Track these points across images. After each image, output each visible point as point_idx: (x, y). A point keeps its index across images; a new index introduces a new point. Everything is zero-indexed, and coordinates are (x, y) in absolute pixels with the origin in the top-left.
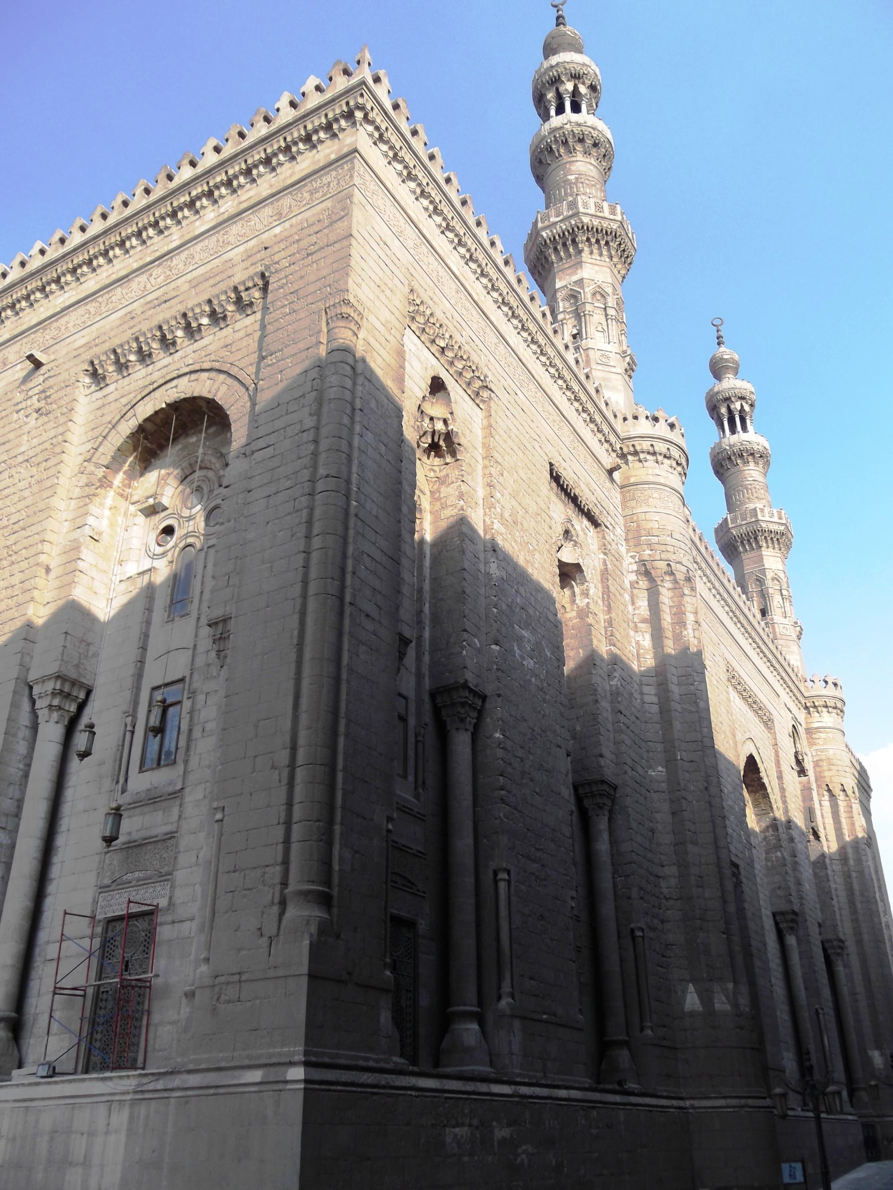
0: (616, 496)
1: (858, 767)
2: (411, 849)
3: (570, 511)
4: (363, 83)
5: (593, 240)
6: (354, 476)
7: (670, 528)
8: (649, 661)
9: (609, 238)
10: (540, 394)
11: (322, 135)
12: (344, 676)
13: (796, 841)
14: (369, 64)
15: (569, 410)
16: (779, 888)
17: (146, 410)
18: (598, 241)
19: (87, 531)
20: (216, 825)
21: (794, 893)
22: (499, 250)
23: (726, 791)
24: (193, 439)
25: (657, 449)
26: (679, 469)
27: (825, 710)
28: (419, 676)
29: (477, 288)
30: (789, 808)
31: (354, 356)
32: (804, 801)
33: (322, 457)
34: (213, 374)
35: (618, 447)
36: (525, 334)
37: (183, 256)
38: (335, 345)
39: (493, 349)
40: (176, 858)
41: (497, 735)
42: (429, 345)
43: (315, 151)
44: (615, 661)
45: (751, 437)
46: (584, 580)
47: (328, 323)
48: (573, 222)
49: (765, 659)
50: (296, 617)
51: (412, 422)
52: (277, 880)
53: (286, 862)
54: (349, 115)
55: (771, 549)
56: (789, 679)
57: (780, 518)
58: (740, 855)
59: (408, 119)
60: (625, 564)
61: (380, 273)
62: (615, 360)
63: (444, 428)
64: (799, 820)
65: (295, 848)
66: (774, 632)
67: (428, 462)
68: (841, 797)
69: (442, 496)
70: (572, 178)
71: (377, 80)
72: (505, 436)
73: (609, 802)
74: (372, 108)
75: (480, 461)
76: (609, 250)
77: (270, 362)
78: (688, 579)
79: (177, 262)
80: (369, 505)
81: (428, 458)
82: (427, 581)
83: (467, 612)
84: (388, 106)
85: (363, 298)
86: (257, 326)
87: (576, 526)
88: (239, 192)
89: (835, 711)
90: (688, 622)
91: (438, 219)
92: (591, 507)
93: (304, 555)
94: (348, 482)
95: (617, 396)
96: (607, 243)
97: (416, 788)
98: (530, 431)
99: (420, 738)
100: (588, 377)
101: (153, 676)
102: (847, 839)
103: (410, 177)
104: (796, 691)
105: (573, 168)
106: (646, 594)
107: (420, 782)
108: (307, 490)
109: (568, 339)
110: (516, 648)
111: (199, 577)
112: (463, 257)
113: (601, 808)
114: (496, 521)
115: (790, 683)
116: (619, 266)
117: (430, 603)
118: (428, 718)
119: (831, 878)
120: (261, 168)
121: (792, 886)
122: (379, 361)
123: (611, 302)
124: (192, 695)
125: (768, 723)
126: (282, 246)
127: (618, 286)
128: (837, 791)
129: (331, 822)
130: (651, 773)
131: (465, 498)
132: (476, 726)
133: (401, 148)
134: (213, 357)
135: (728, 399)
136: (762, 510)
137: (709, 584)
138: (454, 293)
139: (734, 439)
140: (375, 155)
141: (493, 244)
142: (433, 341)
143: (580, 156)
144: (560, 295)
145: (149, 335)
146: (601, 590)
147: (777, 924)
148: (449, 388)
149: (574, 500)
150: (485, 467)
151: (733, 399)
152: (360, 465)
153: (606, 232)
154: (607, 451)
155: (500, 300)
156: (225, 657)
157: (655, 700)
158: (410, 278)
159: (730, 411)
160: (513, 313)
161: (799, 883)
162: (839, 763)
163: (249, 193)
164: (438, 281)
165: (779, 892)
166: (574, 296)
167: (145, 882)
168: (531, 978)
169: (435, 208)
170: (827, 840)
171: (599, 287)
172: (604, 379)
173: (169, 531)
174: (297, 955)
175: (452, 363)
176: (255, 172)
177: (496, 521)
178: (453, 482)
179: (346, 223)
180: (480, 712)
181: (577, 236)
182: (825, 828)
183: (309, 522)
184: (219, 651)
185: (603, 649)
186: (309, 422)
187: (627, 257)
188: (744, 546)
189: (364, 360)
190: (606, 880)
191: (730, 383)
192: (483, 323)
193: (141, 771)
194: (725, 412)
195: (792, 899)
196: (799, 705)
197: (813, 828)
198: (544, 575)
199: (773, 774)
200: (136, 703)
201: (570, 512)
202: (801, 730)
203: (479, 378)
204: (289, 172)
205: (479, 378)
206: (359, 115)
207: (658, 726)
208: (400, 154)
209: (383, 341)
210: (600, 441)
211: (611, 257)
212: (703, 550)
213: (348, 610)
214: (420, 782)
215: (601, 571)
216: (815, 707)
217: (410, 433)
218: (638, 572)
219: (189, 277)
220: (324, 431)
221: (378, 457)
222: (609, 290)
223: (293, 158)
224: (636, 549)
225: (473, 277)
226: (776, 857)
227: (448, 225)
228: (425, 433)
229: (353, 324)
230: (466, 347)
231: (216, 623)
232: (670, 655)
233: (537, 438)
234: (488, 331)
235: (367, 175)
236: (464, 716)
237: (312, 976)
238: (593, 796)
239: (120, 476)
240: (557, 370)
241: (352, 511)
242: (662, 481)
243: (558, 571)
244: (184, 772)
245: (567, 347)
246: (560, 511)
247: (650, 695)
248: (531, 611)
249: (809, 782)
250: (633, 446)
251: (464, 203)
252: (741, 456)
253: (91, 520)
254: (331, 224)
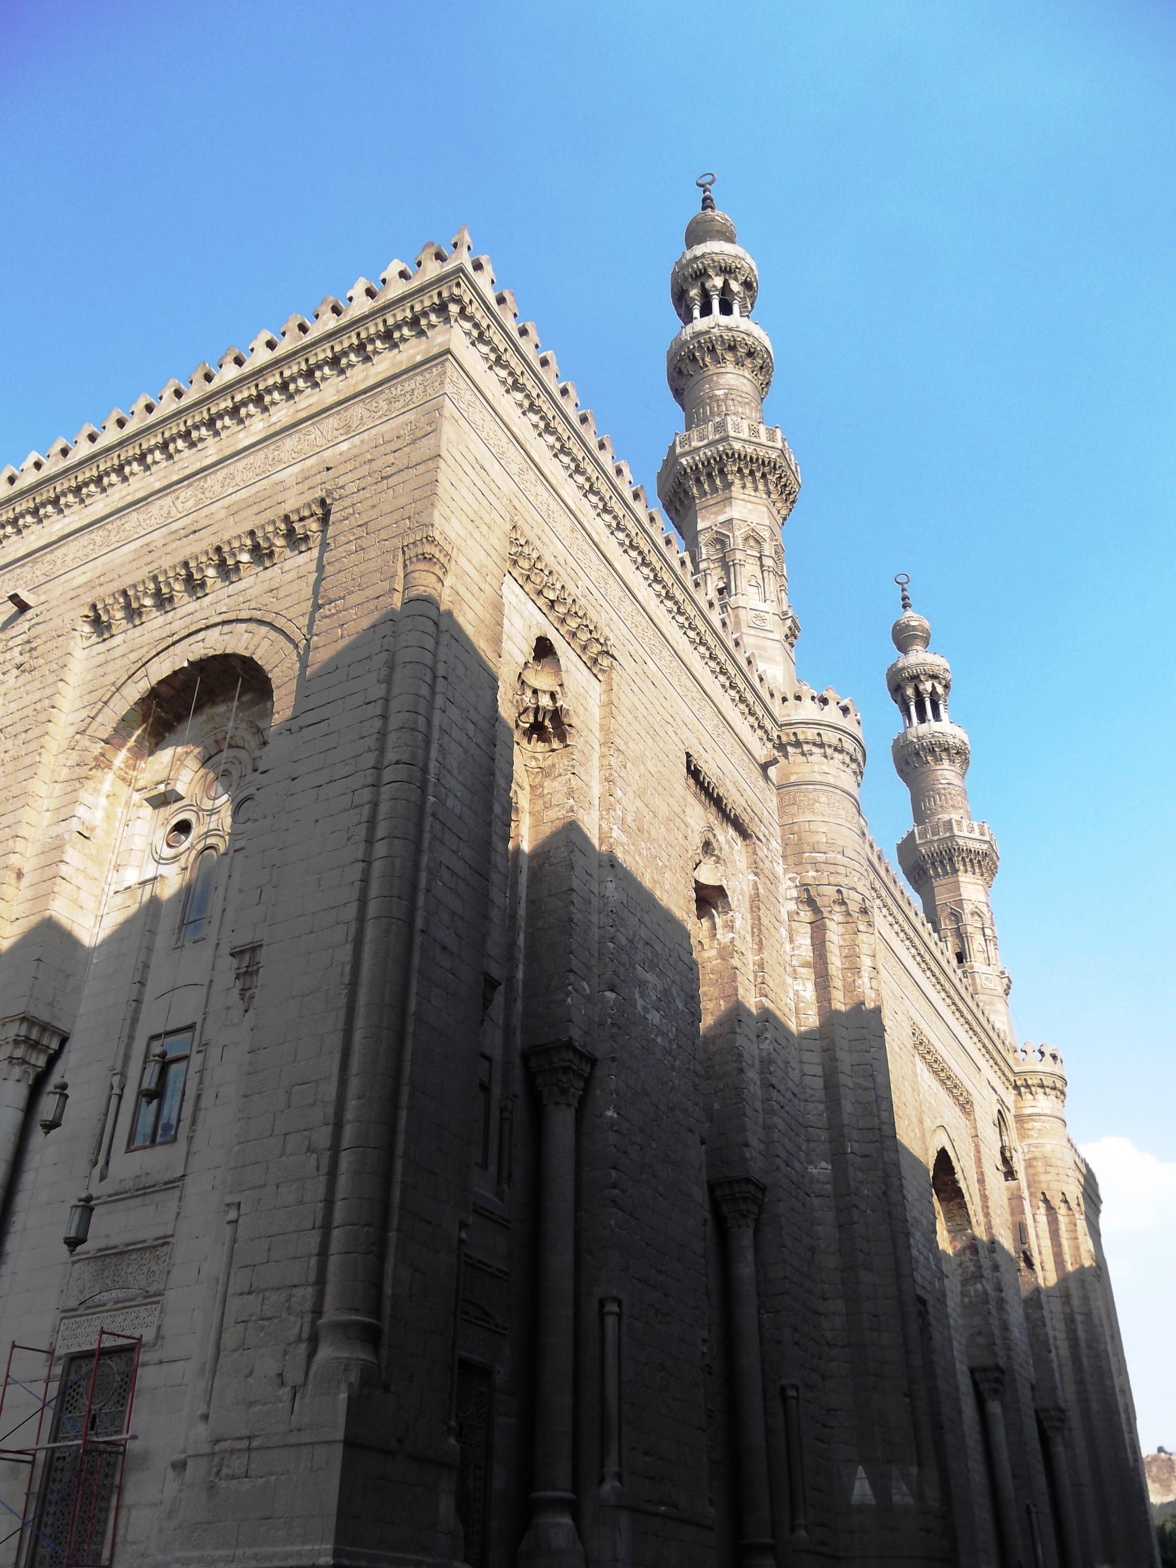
0: (772, 800)
1: (1084, 1171)
2: (490, 1267)
3: (712, 817)
4: (460, 270)
5: (746, 471)
6: (433, 766)
7: (841, 843)
8: (812, 1020)
9: (767, 469)
10: (676, 663)
11: (406, 331)
12: (410, 1028)
13: (1001, 1269)
14: (469, 248)
15: (713, 685)
16: (979, 1334)
17: (162, 669)
18: (752, 473)
19: (75, 824)
20: (229, 1228)
21: (998, 1342)
22: (627, 480)
23: (909, 1197)
24: (221, 709)
25: (825, 739)
26: (854, 766)
27: (1040, 1090)
28: (508, 1030)
29: (598, 527)
30: (993, 1222)
31: (438, 609)
32: (1012, 1214)
33: (392, 738)
34: (252, 626)
35: (775, 734)
36: (658, 587)
37: (221, 475)
38: (414, 593)
39: (616, 604)
40: (169, 1272)
41: (610, 1113)
42: (534, 597)
43: (396, 351)
44: (767, 1017)
45: (945, 727)
46: (728, 908)
47: (405, 566)
48: (721, 449)
49: (962, 1020)
50: (349, 947)
51: (510, 696)
52: (308, 1306)
53: (320, 1282)
54: (441, 309)
55: (970, 874)
56: (994, 1048)
57: (982, 834)
58: (929, 1288)
59: (515, 315)
60: (782, 888)
61: (476, 506)
62: (772, 622)
63: (551, 703)
64: (1006, 1241)
65: (334, 1262)
66: (974, 984)
67: (529, 747)
68: (1062, 1210)
69: (546, 792)
70: (719, 393)
71: (478, 266)
72: (630, 717)
73: (755, 1210)
74: (471, 301)
75: (597, 747)
76: (766, 485)
77: (328, 613)
78: (864, 911)
79: (214, 482)
80: (450, 802)
81: (529, 742)
82: (523, 905)
83: (574, 947)
84: (492, 300)
85: (452, 535)
86: (313, 566)
87: (718, 837)
88: (297, 398)
89: (1053, 1092)
90: (863, 968)
91: (551, 439)
92: (738, 811)
93: (361, 865)
94: (425, 770)
95: (775, 668)
96: (764, 476)
97: (499, 1182)
98: (662, 711)
99: (507, 1115)
100: (737, 644)
101: (152, 1021)
103: (517, 386)
104: (1002, 1064)
105: (722, 381)
106: (808, 928)
107: (505, 1174)
108: (369, 781)
109: (713, 594)
110: (637, 996)
111: (221, 890)
112: (581, 488)
113: (744, 1216)
114: (615, 827)
115: (995, 1054)
116: (779, 505)
117: (526, 932)
118: (518, 1087)
119: (1048, 1322)
120: (326, 370)
121: (996, 1331)
122: (470, 615)
123: (768, 549)
124: (204, 1048)
125: (966, 1106)
126: (350, 466)
127: (777, 530)
128: (1056, 1202)
129: (384, 1227)
130: (811, 1169)
131: (576, 796)
132: (582, 1101)
133: (506, 350)
134: (253, 605)
135: (915, 678)
136: (959, 823)
137: (890, 918)
138: (568, 532)
139: (923, 729)
140: (473, 358)
141: (619, 472)
142: (540, 593)
143: (730, 367)
144: (702, 539)
145: (171, 574)
146: (750, 922)
147: (975, 1384)
148: (559, 652)
149: (716, 802)
150: (603, 756)
151: (922, 678)
152: (442, 749)
153: (763, 461)
154: (761, 739)
155: (627, 543)
156: (252, 997)
157: (819, 1070)
158: (514, 512)
159: (918, 693)
160: (644, 559)
161: (1005, 1327)
162: (1059, 1163)
163: (310, 400)
164: (549, 516)
166: (720, 541)
167: (123, 1305)
168: (646, 1453)
169: (547, 425)
170: (1043, 1268)
171: (753, 530)
172: (758, 647)
173: (183, 827)
174: (330, 1413)
175: (563, 621)
176: (318, 374)
177: (615, 827)
178: (560, 775)
179: (432, 441)
180: (588, 1081)
181: (726, 465)
182: (1040, 1253)
183: (372, 822)
184: (242, 990)
185: (752, 1001)
186: (378, 691)
187: (790, 494)
188: (935, 869)
189: (449, 614)
190: (748, 1315)
191: (918, 657)
192: (604, 570)
193: (128, 1150)
194: (912, 694)
195: (997, 1349)
196: (1007, 1084)
197: (1024, 1253)
198: (678, 901)
199: (973, 1175)
200: (127, 1058)
201: (712, 819)
202: (1009, 1117)
203: (597, 640)
204: (361, 375)
205: (597, 640)
206: (454, 309)
207: (821, 1107)
208: (504, 358)
209: (476, 590)
210: (752, 727)
211: (769, 493)
212: (883, 873)
213: (418, 940)
214: (505, 1174)
215: (751, 896)
216: (1028, 1086)
217: (507, 711)
218: (798, 900)
219: (227, 501)
220: (395, 705)
221: (464, 739)
222: (766, 534)
223: (367, 359)
224: (798, 869)
225: (593, 513)
226: (976, 1290)
227: (563, 446)
228: (526, 710)
229: (437, 567)
230: (582, 601)
231: (242, 952)
232: (838, 1012)
233: (671, 720)
234: (611, 580)
235: (461, 381)
236: (566, 1086)
237: (350, 1444)
238: (736, 1199)
239: (123, 754)
240: (698, 634)
241: (429, 809)
242: (832, 780)
243: (694, 895)
244: (188, 1153)
245: (711, 605)
246: (698, 816)
247: (813, 1065)
248: (658, 947)
249: (1019, 1189)
250: (795, 734)
251: (584, 419)
252: (932, 752)
253: (80, 811)
254: (414, 442)
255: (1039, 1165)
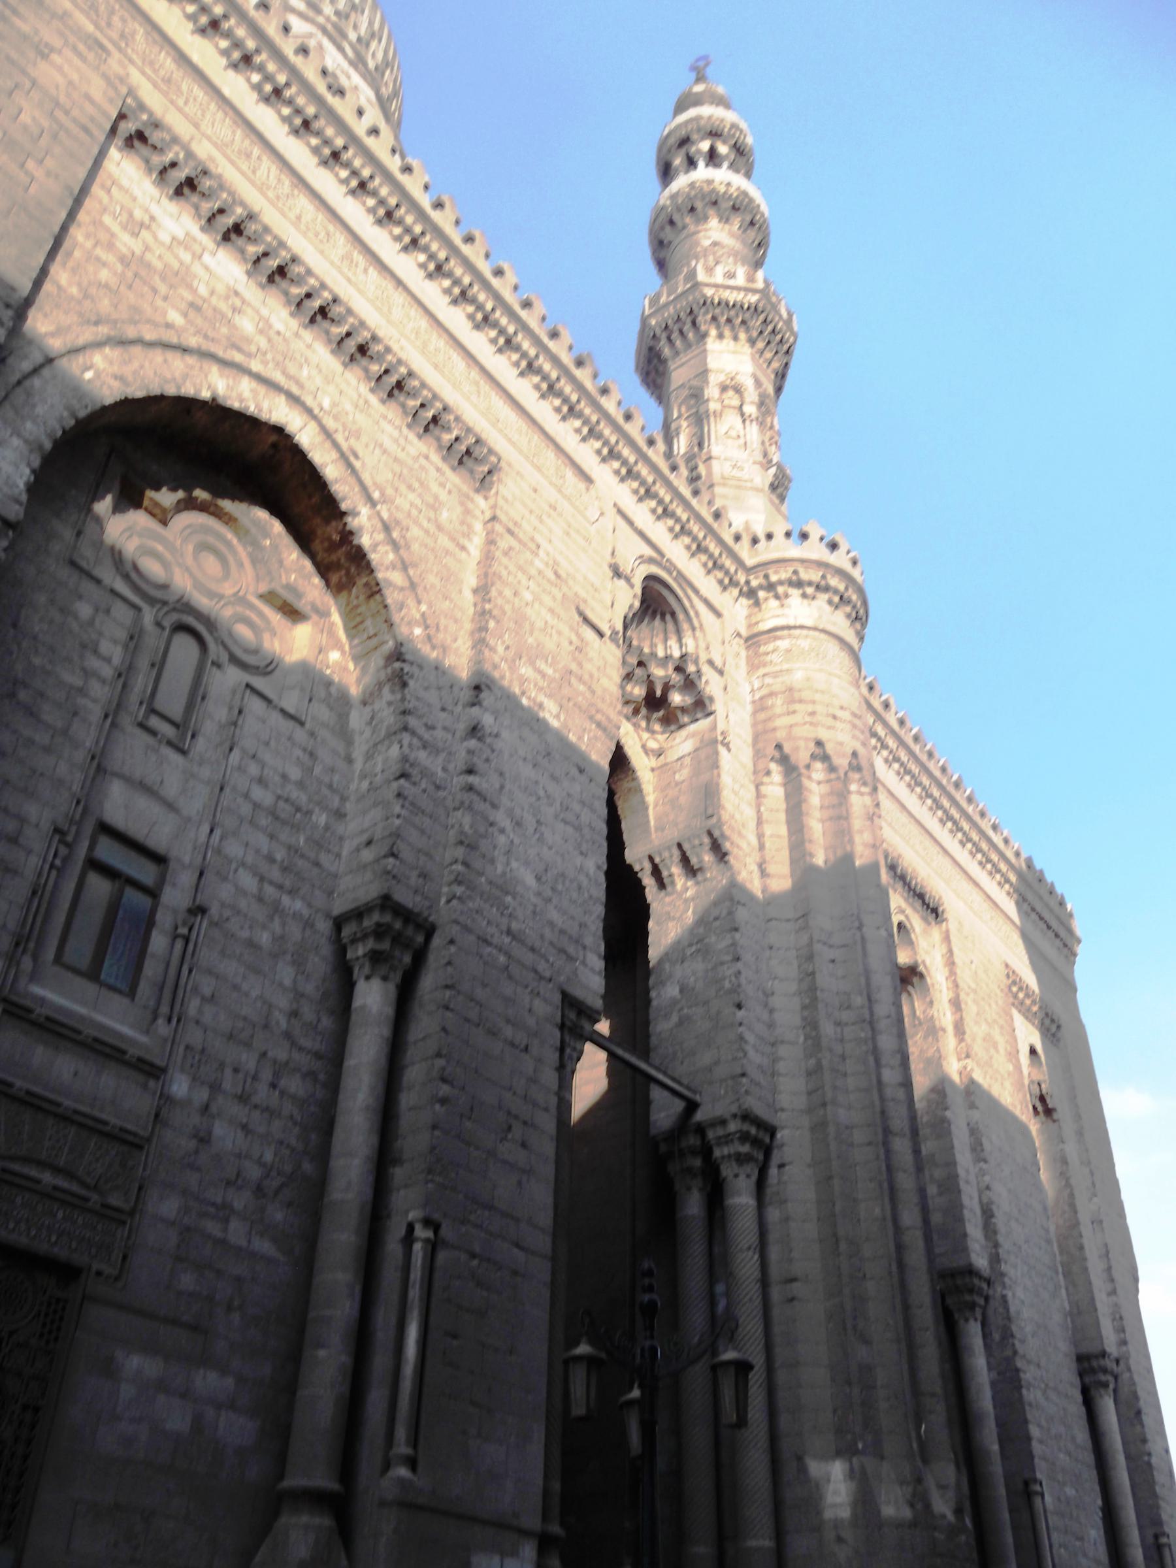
27: (795, 593)
55: (728, 343)
57: (751, 279)
102: (819, 860)
128: (802, 756)
165: (367, 855)
216: (771, 587)
255: (778, 704)
